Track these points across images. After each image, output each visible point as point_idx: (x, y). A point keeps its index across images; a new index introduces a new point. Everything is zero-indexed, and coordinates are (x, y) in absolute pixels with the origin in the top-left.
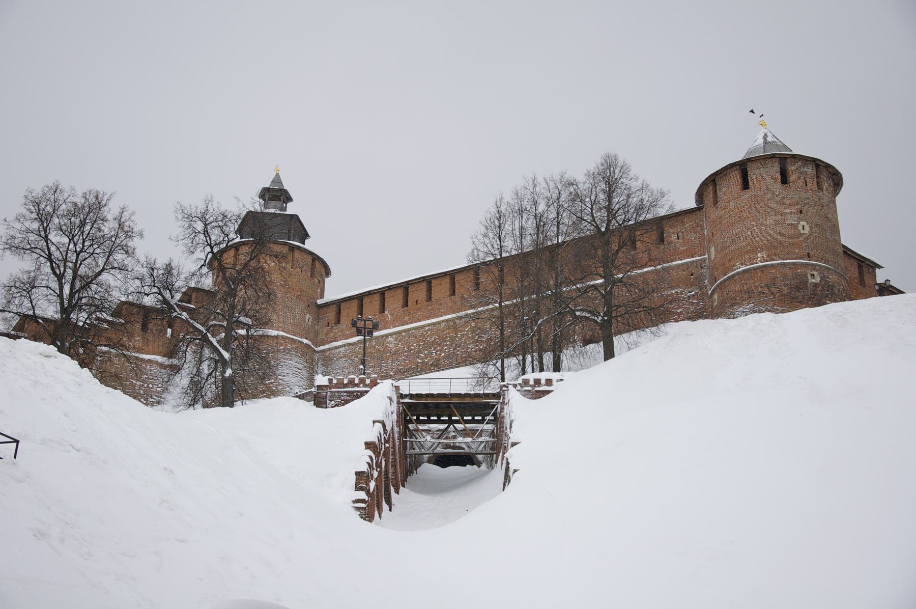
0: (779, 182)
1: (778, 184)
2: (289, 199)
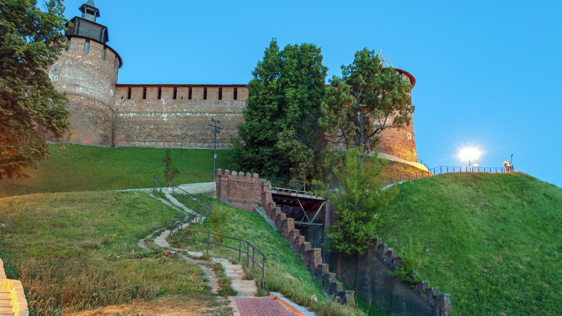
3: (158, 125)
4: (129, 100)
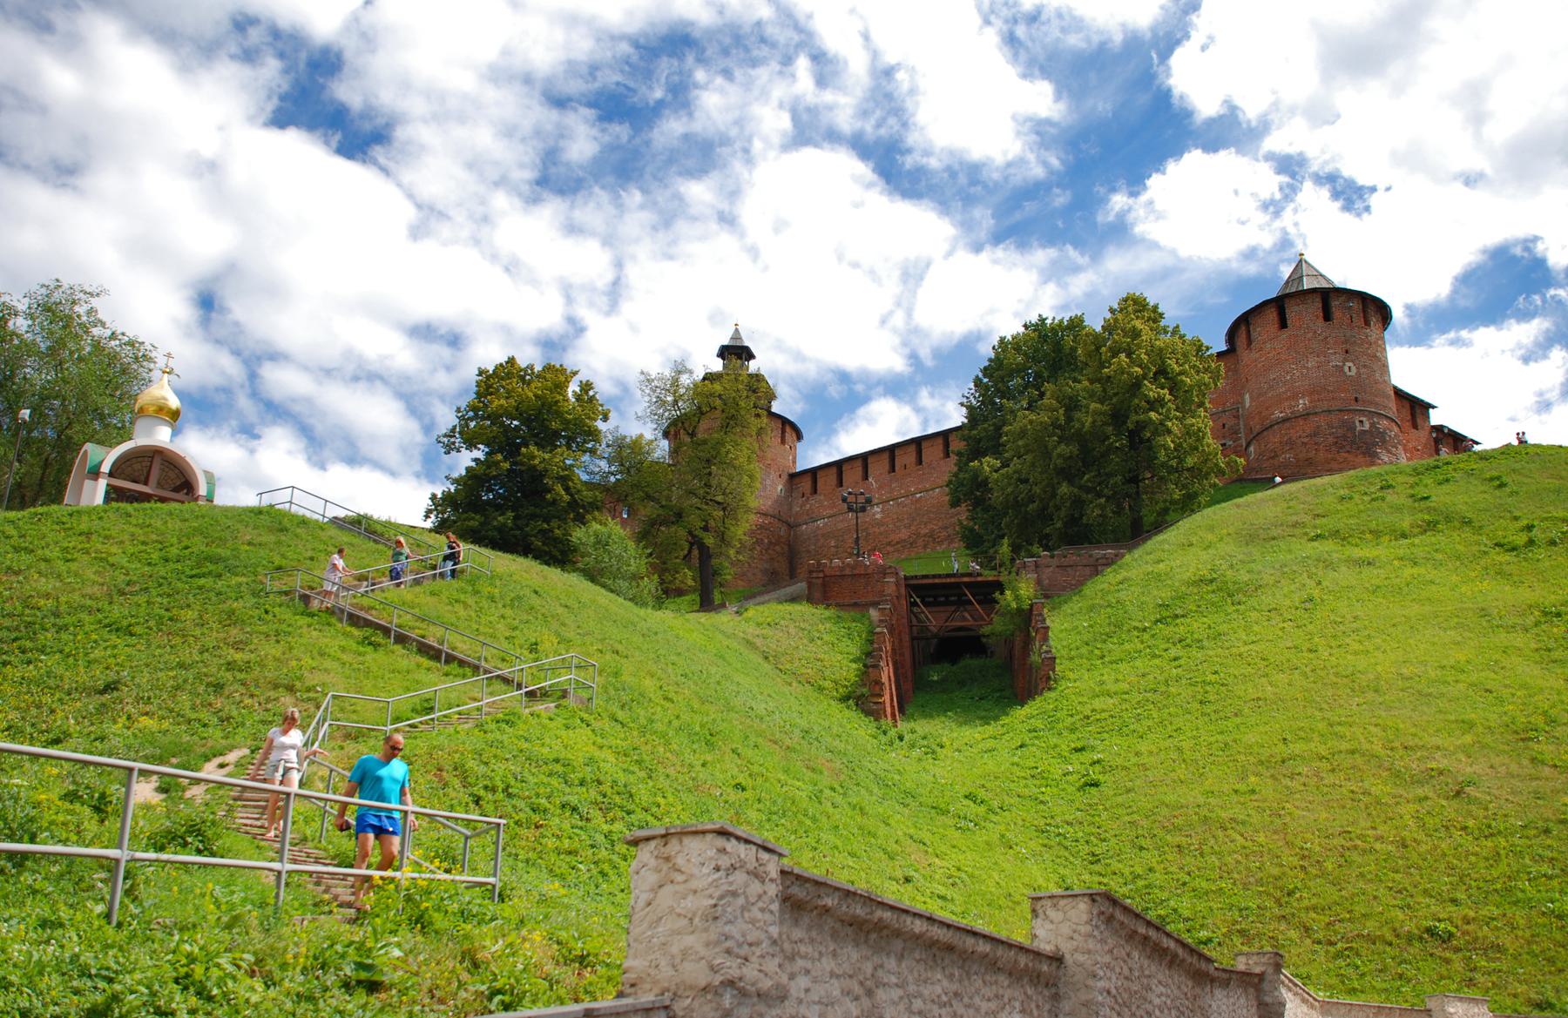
0: (1321, 319)
1: (1320, 322)
2: (751, 356)
4: (817, 497)
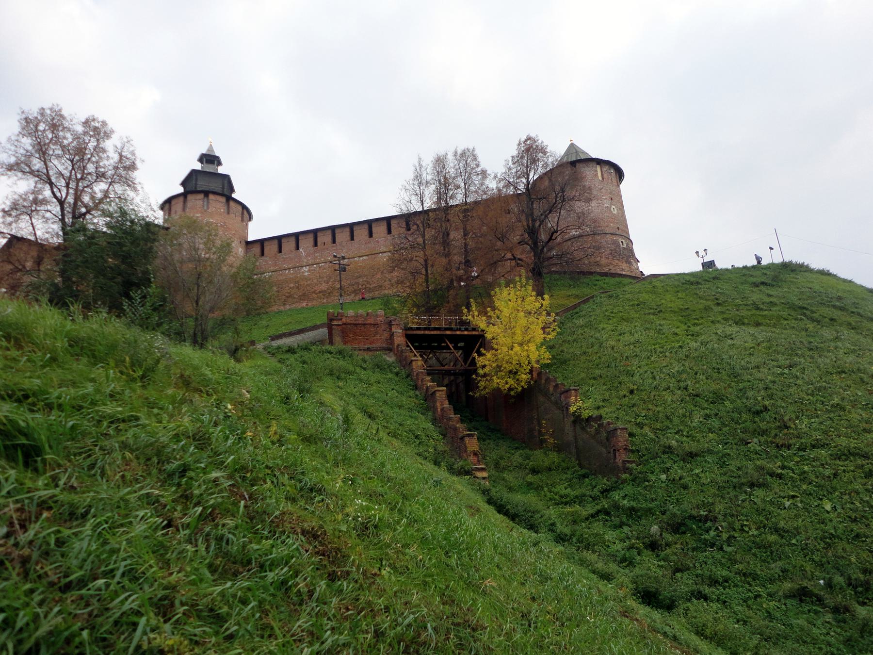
3: (298, 282)
4: (263, 258)
